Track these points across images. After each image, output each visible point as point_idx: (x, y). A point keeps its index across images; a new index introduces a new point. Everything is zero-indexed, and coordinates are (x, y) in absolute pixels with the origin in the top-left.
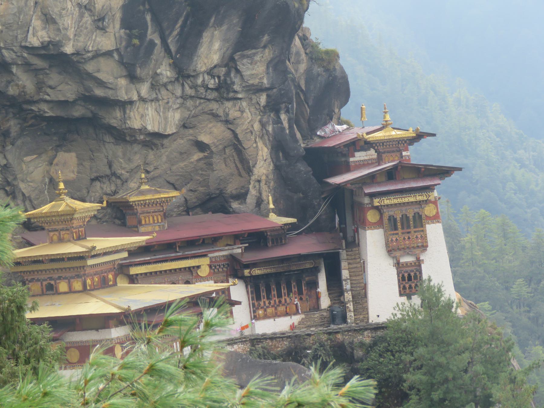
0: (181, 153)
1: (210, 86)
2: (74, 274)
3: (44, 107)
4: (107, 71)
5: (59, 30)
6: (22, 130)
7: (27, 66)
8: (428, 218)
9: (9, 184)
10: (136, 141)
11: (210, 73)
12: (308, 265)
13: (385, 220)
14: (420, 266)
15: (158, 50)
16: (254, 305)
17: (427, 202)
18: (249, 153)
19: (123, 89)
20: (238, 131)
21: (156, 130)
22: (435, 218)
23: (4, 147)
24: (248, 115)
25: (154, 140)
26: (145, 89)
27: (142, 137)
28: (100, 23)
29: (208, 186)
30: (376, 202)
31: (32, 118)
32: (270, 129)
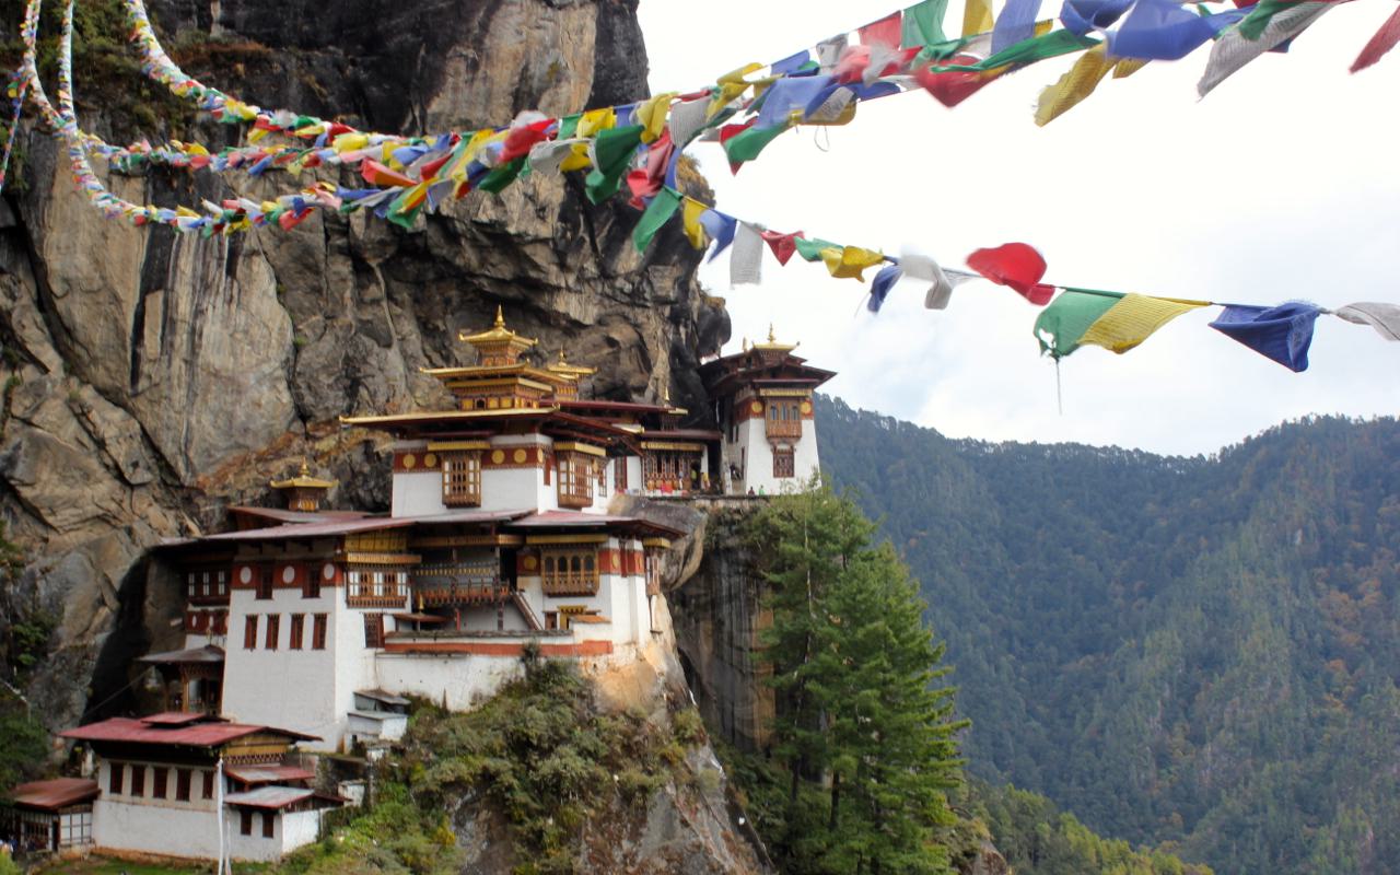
0: (594, 346)
3: (485, 282)
4: (542, 256)
5: (505, 212)
6: (462, 302)
7: (474, 241)
9: (445, 347)
10: (557, 326)
11: (627, 277)
12: (694, 447)
13: (768, 409)
15: (587, 246)
17: (804, 398)
18: (651, 354)
19: (554, 276)
20: (644, 334)
22: (808, 416)
23: (445, 313)
24: (653, 321)
25: (573, 327)
26: (571, 280)
28: (541, 212)
30: (763, 392)
31: (474, 291)
32: (671, 337)
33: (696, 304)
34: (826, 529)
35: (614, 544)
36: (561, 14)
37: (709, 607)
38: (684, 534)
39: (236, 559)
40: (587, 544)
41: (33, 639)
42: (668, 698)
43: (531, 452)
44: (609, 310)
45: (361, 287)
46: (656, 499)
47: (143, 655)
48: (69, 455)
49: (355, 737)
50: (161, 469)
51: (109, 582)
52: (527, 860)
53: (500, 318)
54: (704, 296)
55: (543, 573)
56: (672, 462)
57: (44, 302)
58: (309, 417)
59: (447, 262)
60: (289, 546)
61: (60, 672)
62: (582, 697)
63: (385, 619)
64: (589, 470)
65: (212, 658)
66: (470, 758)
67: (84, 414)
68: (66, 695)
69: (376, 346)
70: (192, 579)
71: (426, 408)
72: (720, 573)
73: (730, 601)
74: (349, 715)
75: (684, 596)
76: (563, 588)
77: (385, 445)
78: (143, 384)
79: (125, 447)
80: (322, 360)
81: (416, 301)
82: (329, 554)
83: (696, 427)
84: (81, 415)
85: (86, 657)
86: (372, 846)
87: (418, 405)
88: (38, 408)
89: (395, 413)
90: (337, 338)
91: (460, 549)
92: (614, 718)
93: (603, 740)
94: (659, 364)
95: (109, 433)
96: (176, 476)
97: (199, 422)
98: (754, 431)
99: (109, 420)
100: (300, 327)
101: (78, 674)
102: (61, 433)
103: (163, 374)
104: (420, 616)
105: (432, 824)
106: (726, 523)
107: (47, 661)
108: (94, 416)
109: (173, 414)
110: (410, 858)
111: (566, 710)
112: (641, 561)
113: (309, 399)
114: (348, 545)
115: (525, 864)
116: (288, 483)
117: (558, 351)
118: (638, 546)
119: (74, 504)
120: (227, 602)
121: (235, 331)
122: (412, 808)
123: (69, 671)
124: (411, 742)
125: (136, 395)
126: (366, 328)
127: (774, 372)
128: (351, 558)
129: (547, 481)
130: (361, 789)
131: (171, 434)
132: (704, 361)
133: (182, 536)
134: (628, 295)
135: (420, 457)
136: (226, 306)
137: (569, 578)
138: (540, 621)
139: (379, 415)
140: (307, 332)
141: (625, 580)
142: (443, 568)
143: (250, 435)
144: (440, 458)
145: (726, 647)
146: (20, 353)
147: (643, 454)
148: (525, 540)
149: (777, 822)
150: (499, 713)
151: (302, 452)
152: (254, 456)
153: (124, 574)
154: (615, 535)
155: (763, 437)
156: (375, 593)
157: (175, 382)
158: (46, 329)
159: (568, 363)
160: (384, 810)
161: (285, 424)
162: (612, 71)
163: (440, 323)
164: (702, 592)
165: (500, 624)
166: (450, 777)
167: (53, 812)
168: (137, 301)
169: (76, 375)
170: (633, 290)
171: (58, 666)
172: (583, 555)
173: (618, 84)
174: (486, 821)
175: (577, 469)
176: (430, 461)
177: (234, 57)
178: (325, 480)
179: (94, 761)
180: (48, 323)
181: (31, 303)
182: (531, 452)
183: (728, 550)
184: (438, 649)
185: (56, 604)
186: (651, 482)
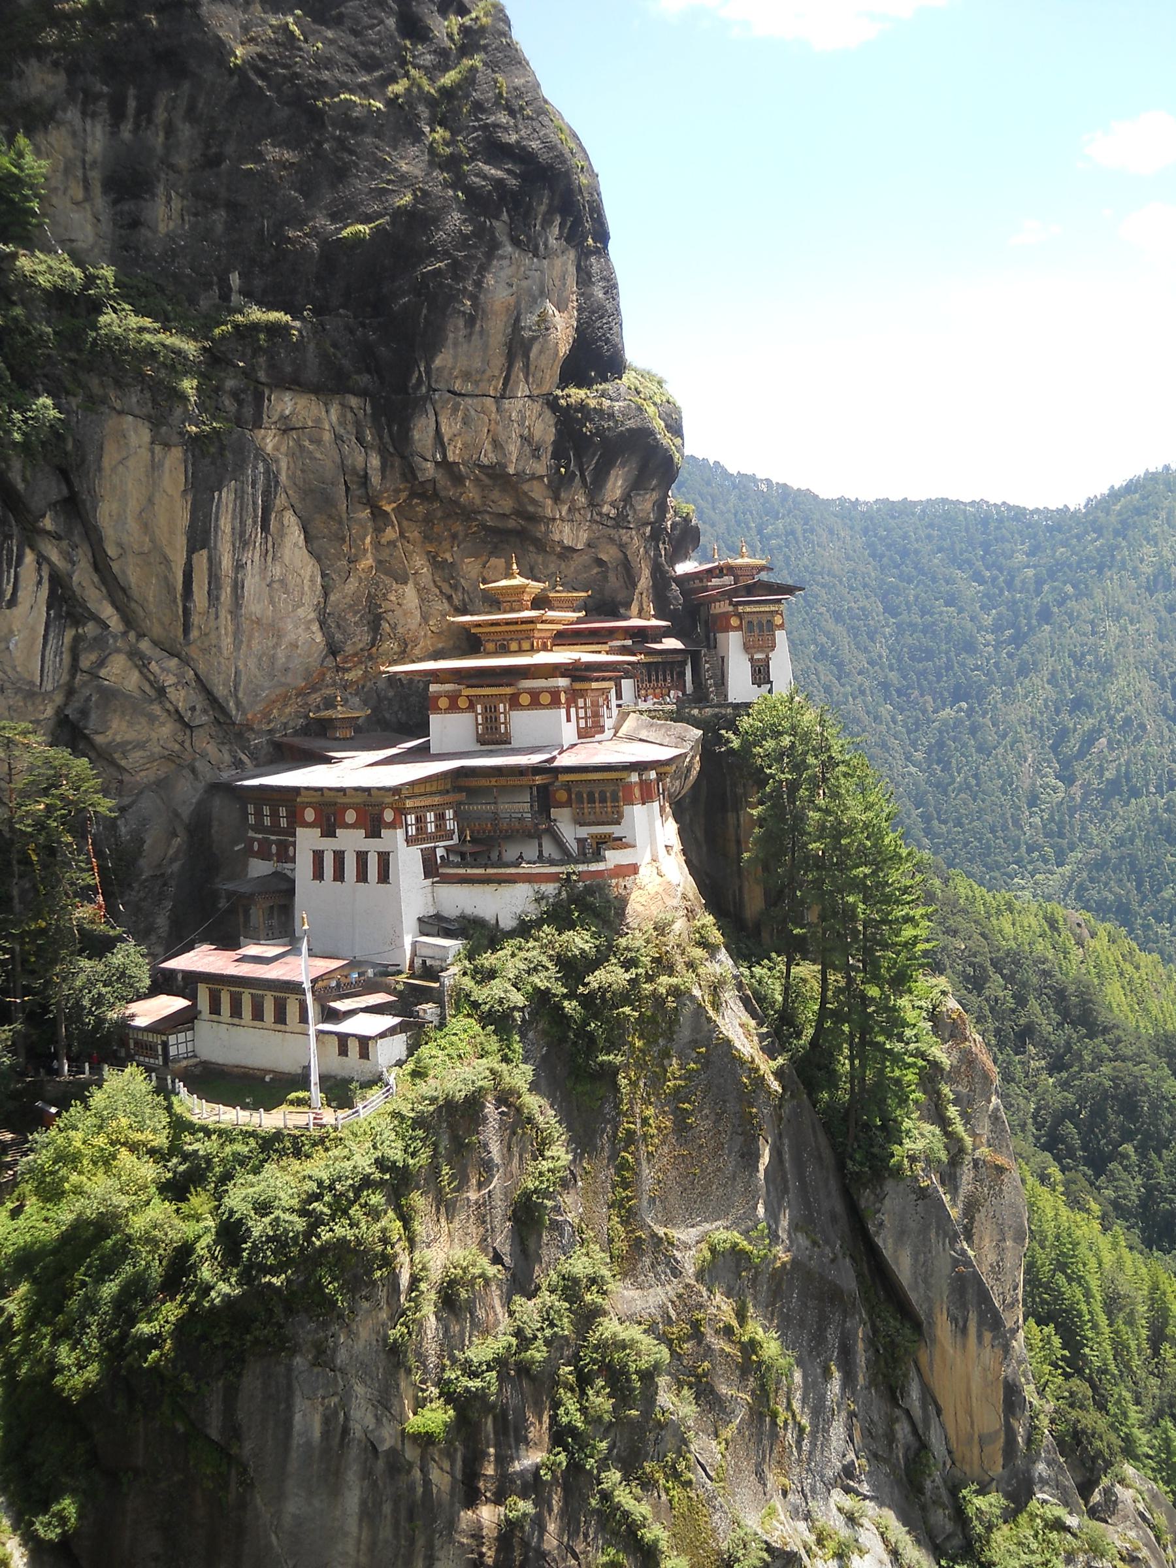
3: (487, 517)
4: (537, 491)
6: (467, 535)
7: (477, 480)
22: (781, 627)
25: (568, 552)
26: (565, 509)
28: (536, 453)
35: (634, 778)
36: (545, 262)
45: (378, 531)
49: (424, 962)
51: (177, 815)
57: (101, 565)
59: (455, 503)
61: (144, 899)
64: (601, 701)
65: (284, 886)
70: (251, 809)
76: (592, 818)
78: (195, 633)
79: (183, 693)
80: (348, 600)
81: (427, 538)
82: (388, 800)
88: (102, 663)
94: (643, 580)
95: (170, 680)
98: (733, 643)
99: (167, 670)
102: (126, 683)
104: (468, 848)
108: (153, 666)
113: (338, 636)
118: (653, 775)
119: (140, 745)
120: (294, 835)
125: (188, 644)
127: (749, 590)
128: (409, 804)
129: (569, 720)
131: (222, 677)
135: (453, 699)
138: (573, 846)
151: (334, 684)
162: (593, 312)
163: (448, 556)
165: (541, 852)
171: (142, 894)
173: (598, 324)
176: (463, 703)
177: (255, 327)
180: (104, 581)
182: (555, 694)
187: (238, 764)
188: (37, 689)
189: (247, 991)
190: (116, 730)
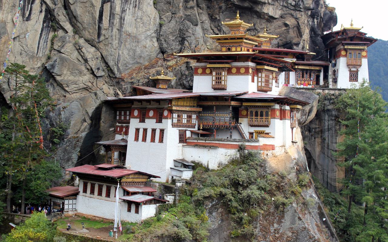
0: (279, 26)
1: (292, 4)
2: (238, 45)
6: (226, 8)
8: (363, 56)
9: (219, 26)
10: (264, 18)
12: (317, 68)
14: (358, 72)
16: (297, 79)
17: (363, 50)
18: (302, 30)
20: (299, 22)
21: (272, 15)
24: (303, 17)
25: (271, 19)
27: (267, 17)
29: (287, 39)
30: (346, 47)
31: (231, 4)
32: (310, 23)
33: (322, 10)
34: (367, 104)
35: (277, 107)
37: (320, 133)
38: (308, 104)
39: (133, 106)
40: (266, 106)
41: (59, 133)
42: (297, 169)
43: (247, 69)
44: (286, 12)
46: (300, 89)
47: (99, 141)
48: (74, 65)
49: (173, 177)
50: (108, 71)
51: (87, 113)
52: (236, 229)
53: (238, 15)
54: (326, 7)
55: (249, 117)
56: (308, 74)
58: (165, 52)
60: (152, 102)
61: (68, 146)
62: (262, 166)
63: (187, 131)
64: (271, 77)
66: (215, 188)
67: (80, 49)
68: (70, 155)
69: (192, 25)
70: (118, 113)
71: (211, 50)
72: (325, 120)
73: (329, 131)
74: (171, 168)
75: (310, 128)
76: (256, 123)
77: (194, 64)
78: (102, 38)
79: (95, 62)
80: (170, 30)
81: (208, 7)
82: (166, 106)
83: (319, 60)
84: (79, 49)
85: (78, 141)
86: (174, 219)
87: (208, 48)
88: (63, 46)
89: (199, 51)
90: (176, 21)
91: (217, 106)
92: (274, 176)
93: (268, 184)
94: (305, 34)
95: (89, 56)
96: (114, 74)
97: (123, 53)
98: (342, 63)
99: (89, 51)
100: (162, 17)
101: (75, 147)
102: (72, 56)
103: (109, 34)
104: (201, 132)
105: (199, 212)
106: (328, 99)
107: (64, 142)
108: (83, 50)
109: (113, 50)
110: (189, 225)
111: (253, 171)
112: (288, 113)
113: (165, 45)
114: (173, 103)
115: (235, 230)
116: (156, 78)
117: (264, 28)
118: (287, 108)
120: (129, 123)
121: (137, 18)
122: (192, 206)
123: (71, 146)
124: (194, 180)
125: (99, 42)
126: (188, 18)
127: (352, 39)
128: (174, 108)
129: (253, 81)
130: (173, 197)
131: (112, 57)
132: (325, 33)
133: (115, 97)
134: (294, 6)
135: (204, 69)
136: (134, 9)
137: (259, 120)
138: (247, 136)
139: (192, 52)
140: (165, 19)
141: (281, 121)
142: (210, 113)
143: (142, 59)
144: (212, 69)
145: (326, 149)
146: (57, 25)
147: (296, 70)
148: (242, 104)
149: (342, 220)
150: (228, 171)
151: (162, 66)
152: (143, 67)
153: (93, 110)
154: (278, 103)
155: (346, 65)
156: (183, 122)
157: (114, 38)
158: (67, 17)
159: (268, 33)
160: (181, 206)
161: (155, 55)
163: (217, 16)
164: (317, 126)
166: (207, 195)
167: (62, 198)
168: (100, 6)
169: (78, 34)
170: (296, 4)
171: (68, 144)
172: (264, 111)
174: (220, 213)
175: (266, 76)
176: (208, 71)
178: (171, 76)
179: (79, 180)
180: (68, 14)
181: (62, 6)
182: (247, 69)
183: (328, 110)
184: (206, 145)
185: (68, 120)
186: (299, 82)
187: (116, 94)
188: (35, 55)
189: (97, 183)
190: (64, 75)
